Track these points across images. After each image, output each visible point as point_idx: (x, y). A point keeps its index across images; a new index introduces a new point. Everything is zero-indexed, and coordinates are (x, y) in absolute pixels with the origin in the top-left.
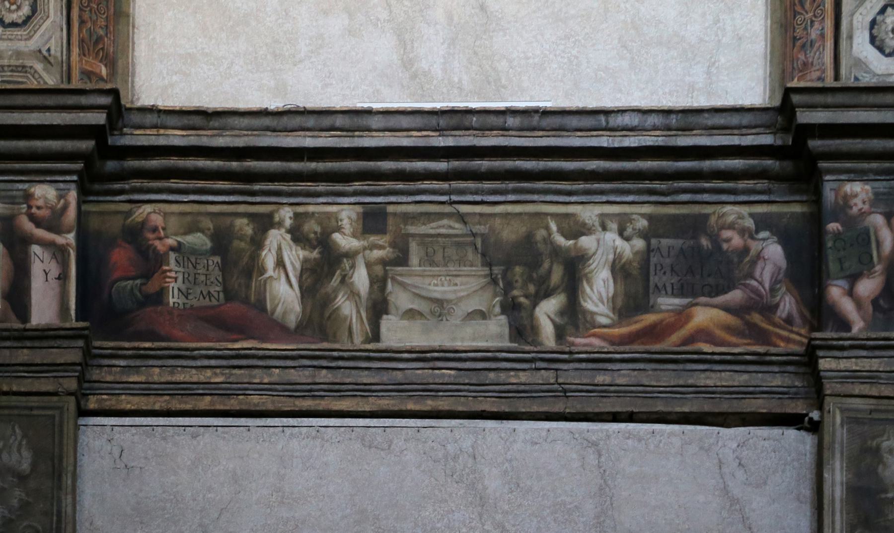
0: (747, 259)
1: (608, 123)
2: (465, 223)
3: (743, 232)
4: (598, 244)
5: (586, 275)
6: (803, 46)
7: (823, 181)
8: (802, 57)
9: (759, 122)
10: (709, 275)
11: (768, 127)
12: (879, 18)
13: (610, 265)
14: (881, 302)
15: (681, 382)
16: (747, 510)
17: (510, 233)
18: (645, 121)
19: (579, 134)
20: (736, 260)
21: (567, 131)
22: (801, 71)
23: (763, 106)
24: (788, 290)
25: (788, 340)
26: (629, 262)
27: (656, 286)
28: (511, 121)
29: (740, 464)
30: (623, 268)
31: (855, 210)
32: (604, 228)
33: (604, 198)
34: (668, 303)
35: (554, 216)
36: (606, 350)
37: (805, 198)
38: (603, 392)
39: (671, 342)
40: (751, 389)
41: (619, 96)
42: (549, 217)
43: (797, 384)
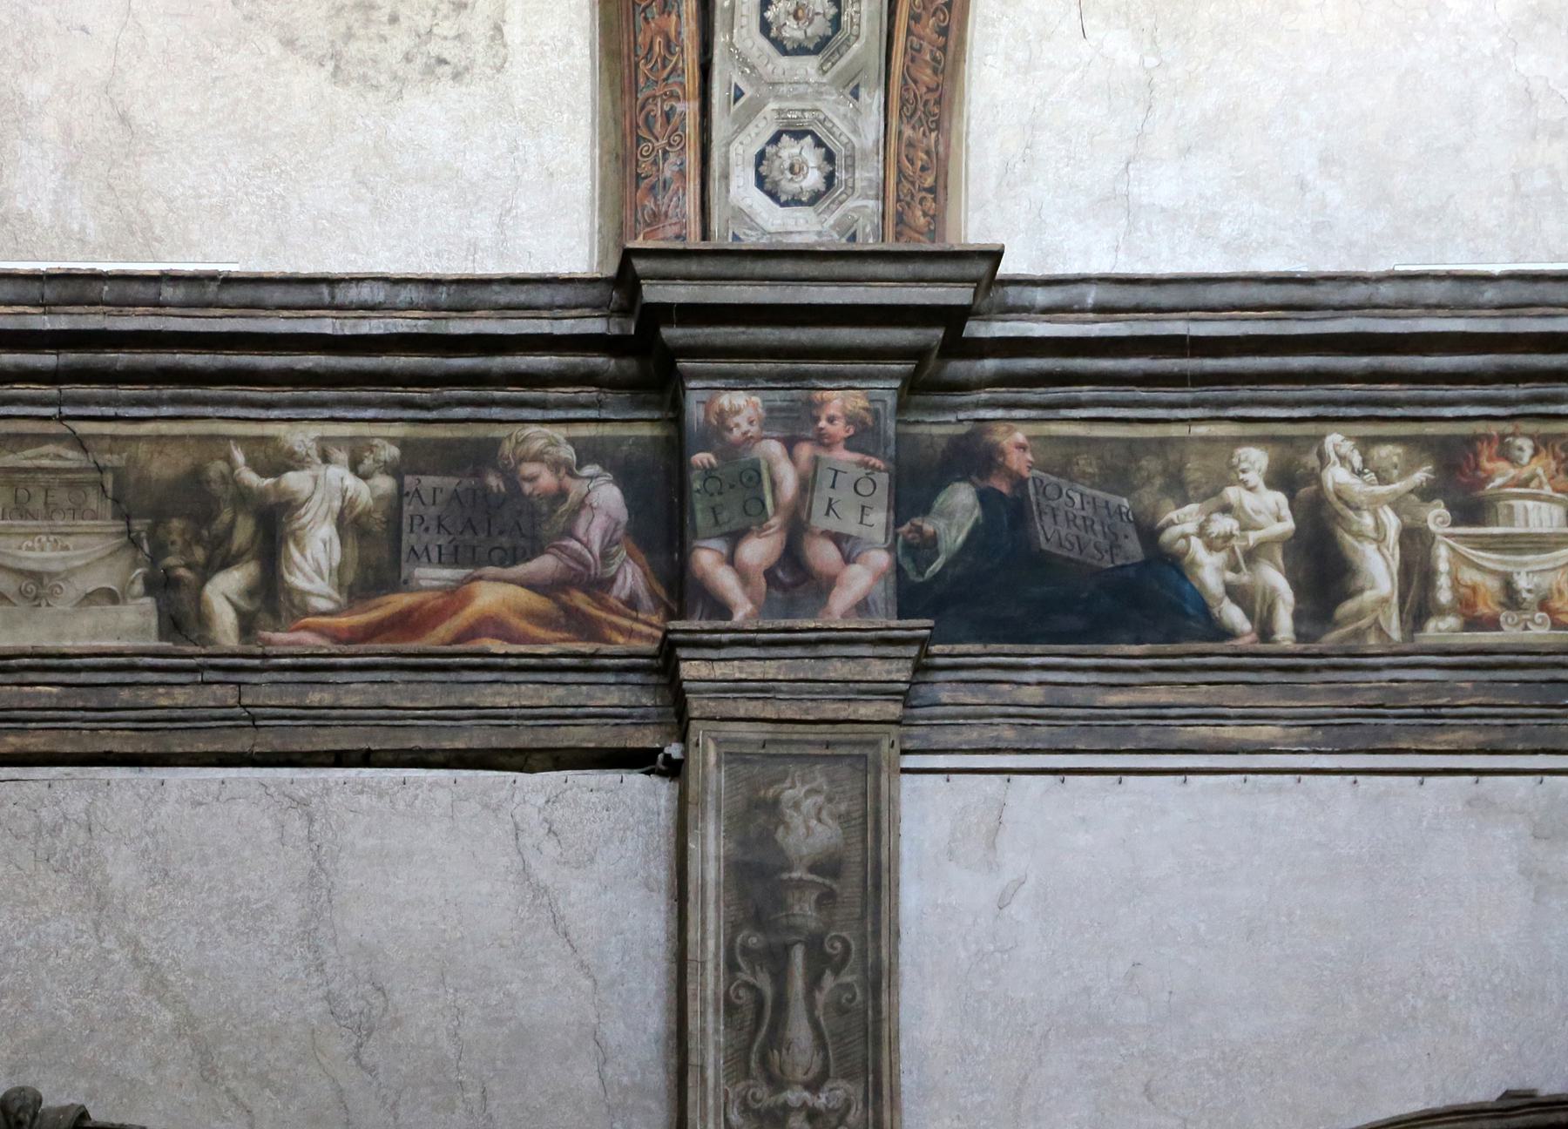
1: (333, 298)
2: (86, 451)
3: (556, 466)
4: (316, 483)
5: (293, 533)
6: (653, 187)
7: (684, 389)
8: (650, 204)
9: (582, 300)
10: (501, 533)
11: (596, 306)
12: (770, 150)
13: (335, 516)
15: (453, 701)
16: (561, 904)
17: (163, 467)
18: (398, 296)
19: (286, 313)
20: (545, 509)
21: (265, 308)
22: (648, 225)
23: (588, 276)
25: (630, 633)
26: (368, 513)
27: (413, 549)
28: (168, 292)
29: (550, 829)
30: (356, 520)
32: (326, 459)
33: (326, 413)
34: (432, 576)
35: (241, 440)
36: (325, 651)
37: (656, 415)
38: (320, 718)
39: (435, 639)
40: (569, 711)
41: (352, 256)
42: (232, 442)
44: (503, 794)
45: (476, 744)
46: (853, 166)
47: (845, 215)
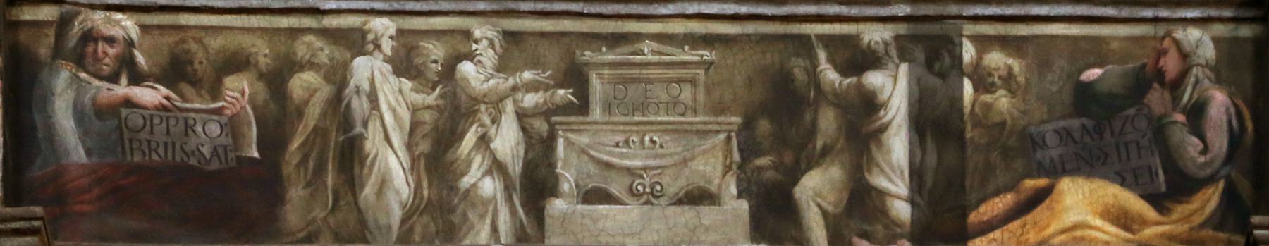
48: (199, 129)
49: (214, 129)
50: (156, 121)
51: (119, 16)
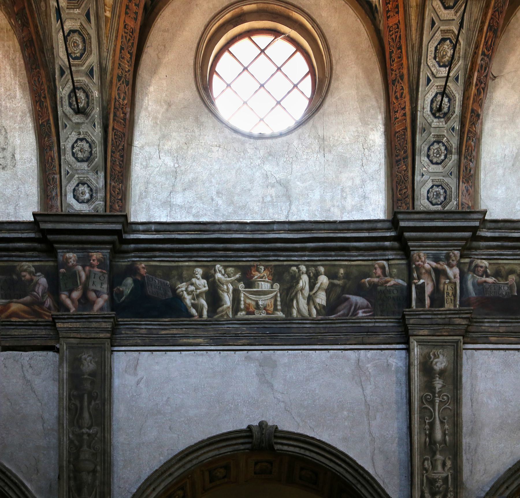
0: (32, 284)
12: (77, 188)
14: (82, 300)
16: (33, 385)
24: (49, 296)
31: (71, 264)
43: (51, 333)
44: (18, 357)
45: (11, 344)
46: (97, 193)
47: (95, 206)
48: (502, 288)
49: (506, 288)
50: (492, 286)
51: (484, 261)
